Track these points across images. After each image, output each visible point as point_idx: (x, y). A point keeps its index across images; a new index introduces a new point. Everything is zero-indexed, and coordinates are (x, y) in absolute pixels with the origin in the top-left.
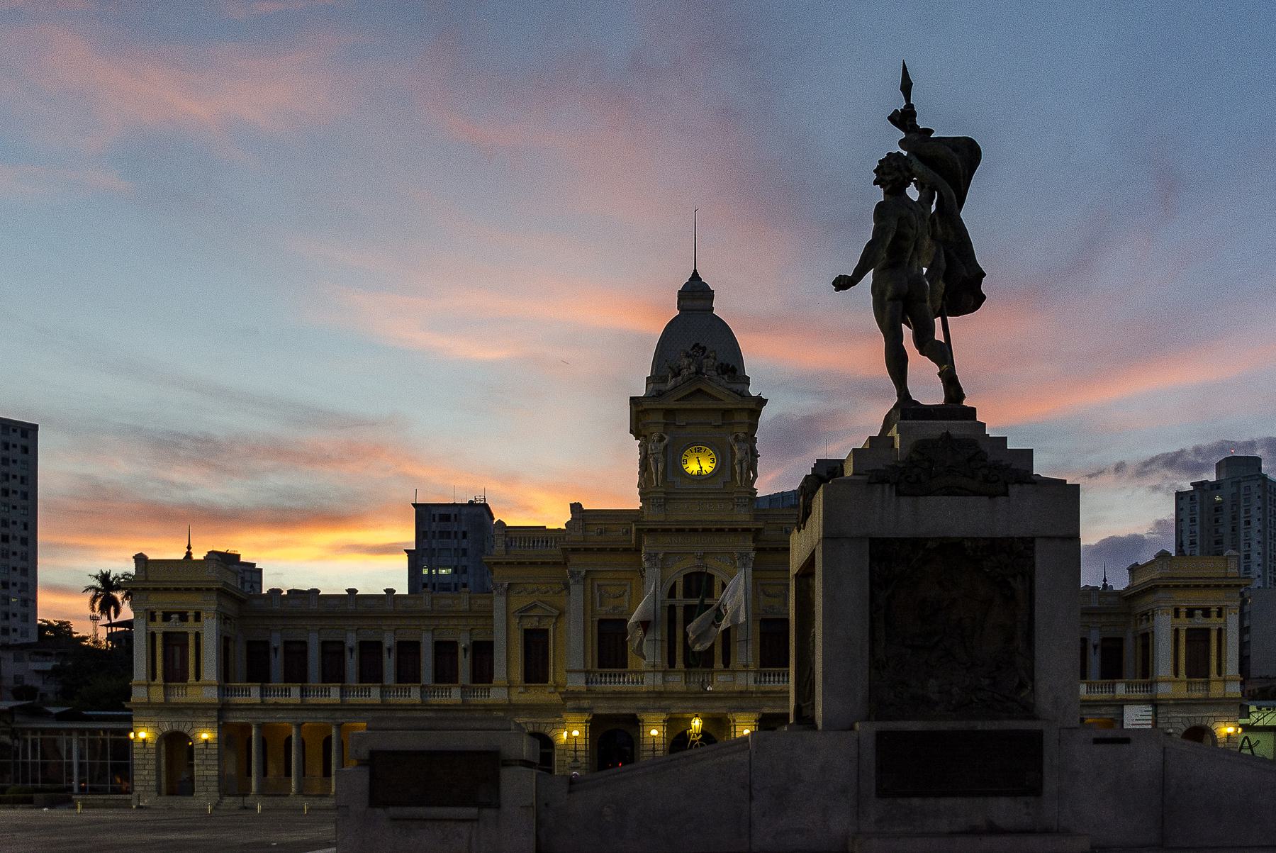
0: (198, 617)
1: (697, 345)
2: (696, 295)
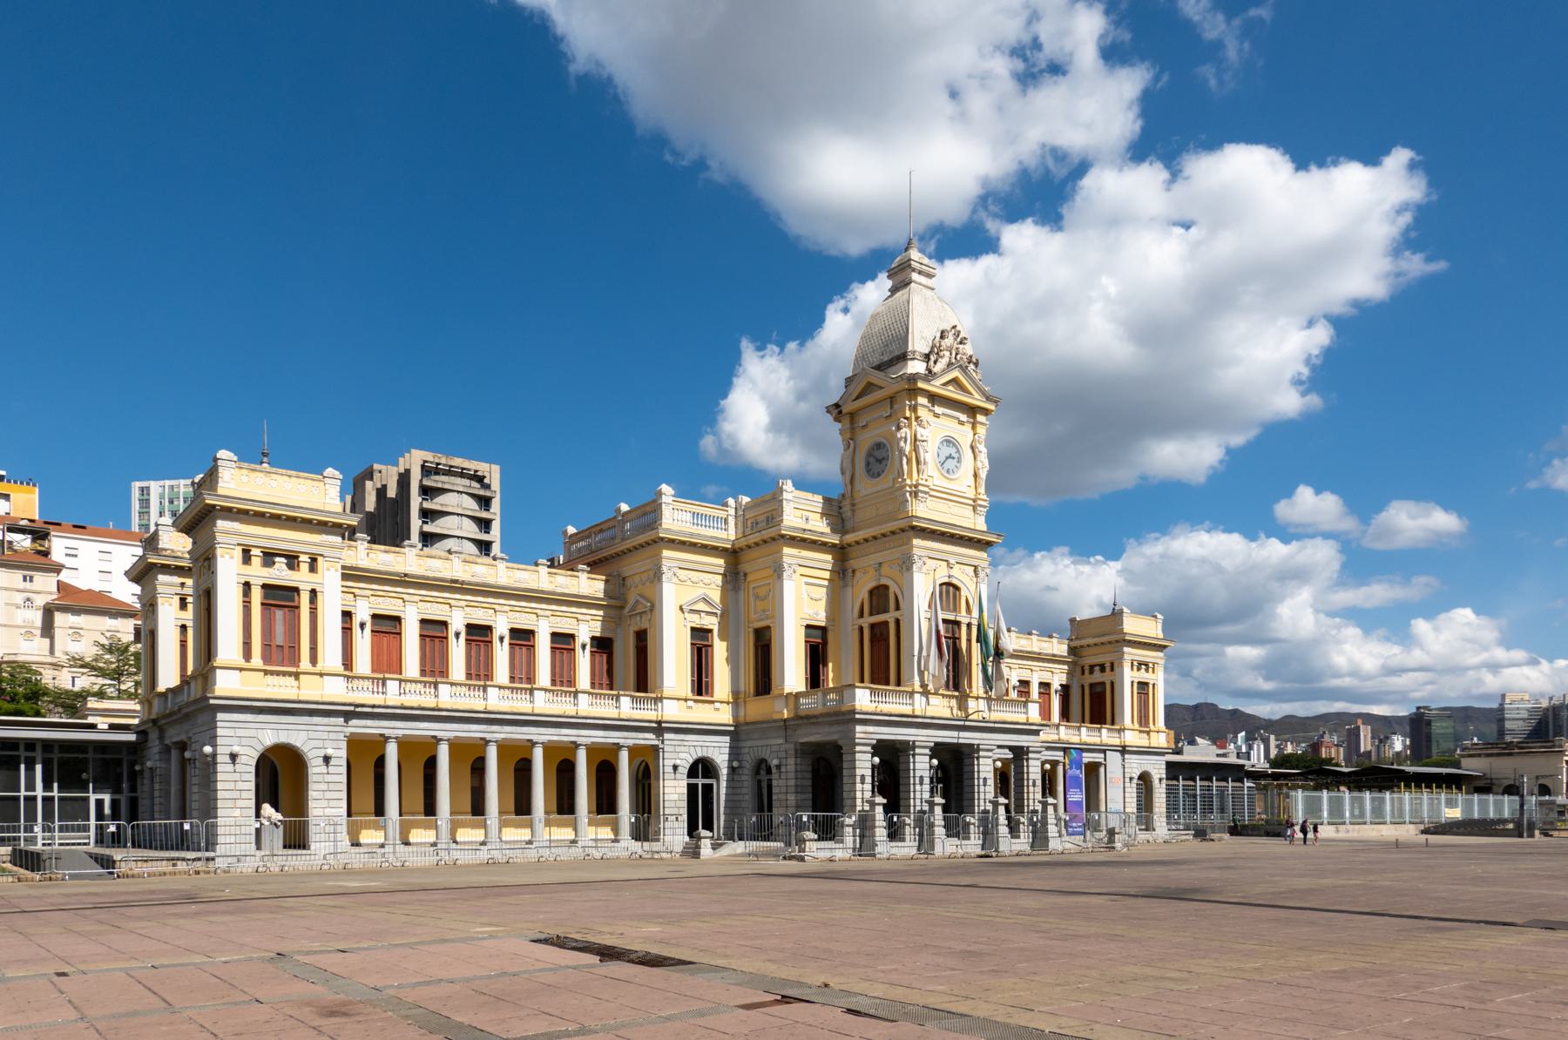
0: (313, 568)
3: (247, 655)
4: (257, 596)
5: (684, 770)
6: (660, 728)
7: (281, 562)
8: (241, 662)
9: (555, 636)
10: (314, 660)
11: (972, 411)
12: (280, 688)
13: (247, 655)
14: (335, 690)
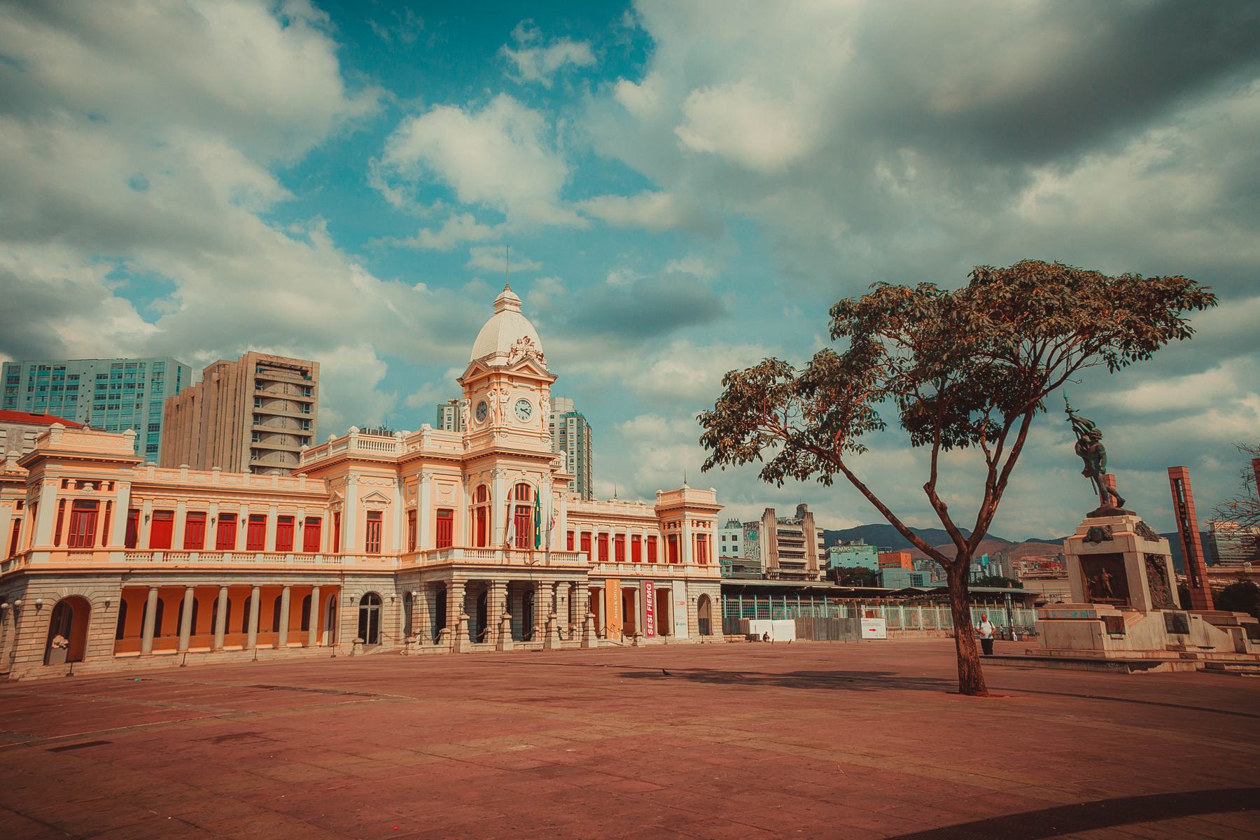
3: (57, 542)
4: (69, 507)
6: (342, 574)
7: (89, 486)
8: (53, 547)
9: (281, 518)
10: (104, 543)
11: (540, 382)
12: (80, 561)
13: (57, 542)
14: (118, 560)
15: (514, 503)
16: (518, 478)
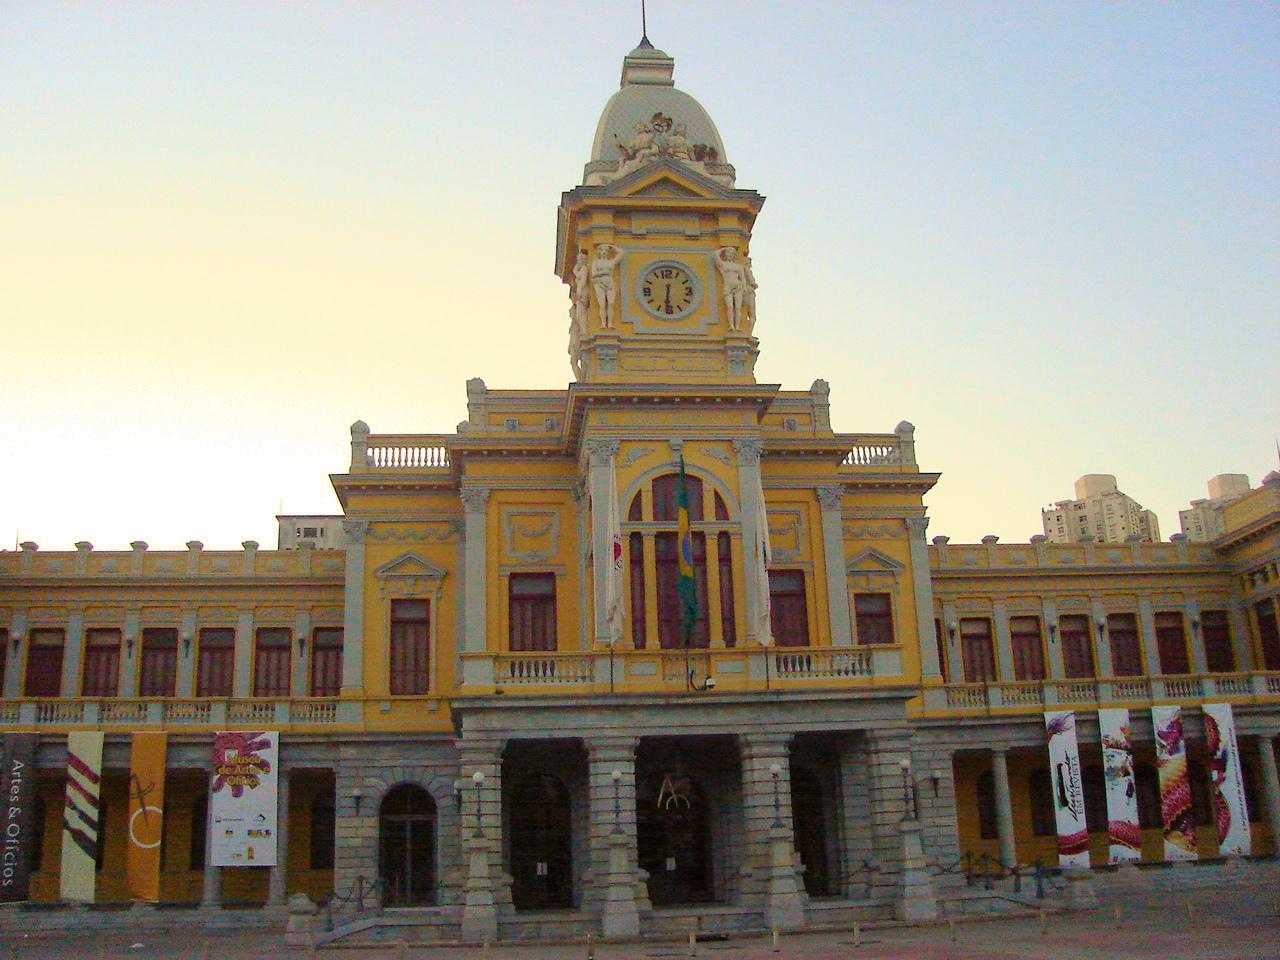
1: (658, 115)
2: (647, 66)
5: (373, 803)
6: (333, 742)
11: (709, 215)
15: (649, 525)
16: (660, 462)
